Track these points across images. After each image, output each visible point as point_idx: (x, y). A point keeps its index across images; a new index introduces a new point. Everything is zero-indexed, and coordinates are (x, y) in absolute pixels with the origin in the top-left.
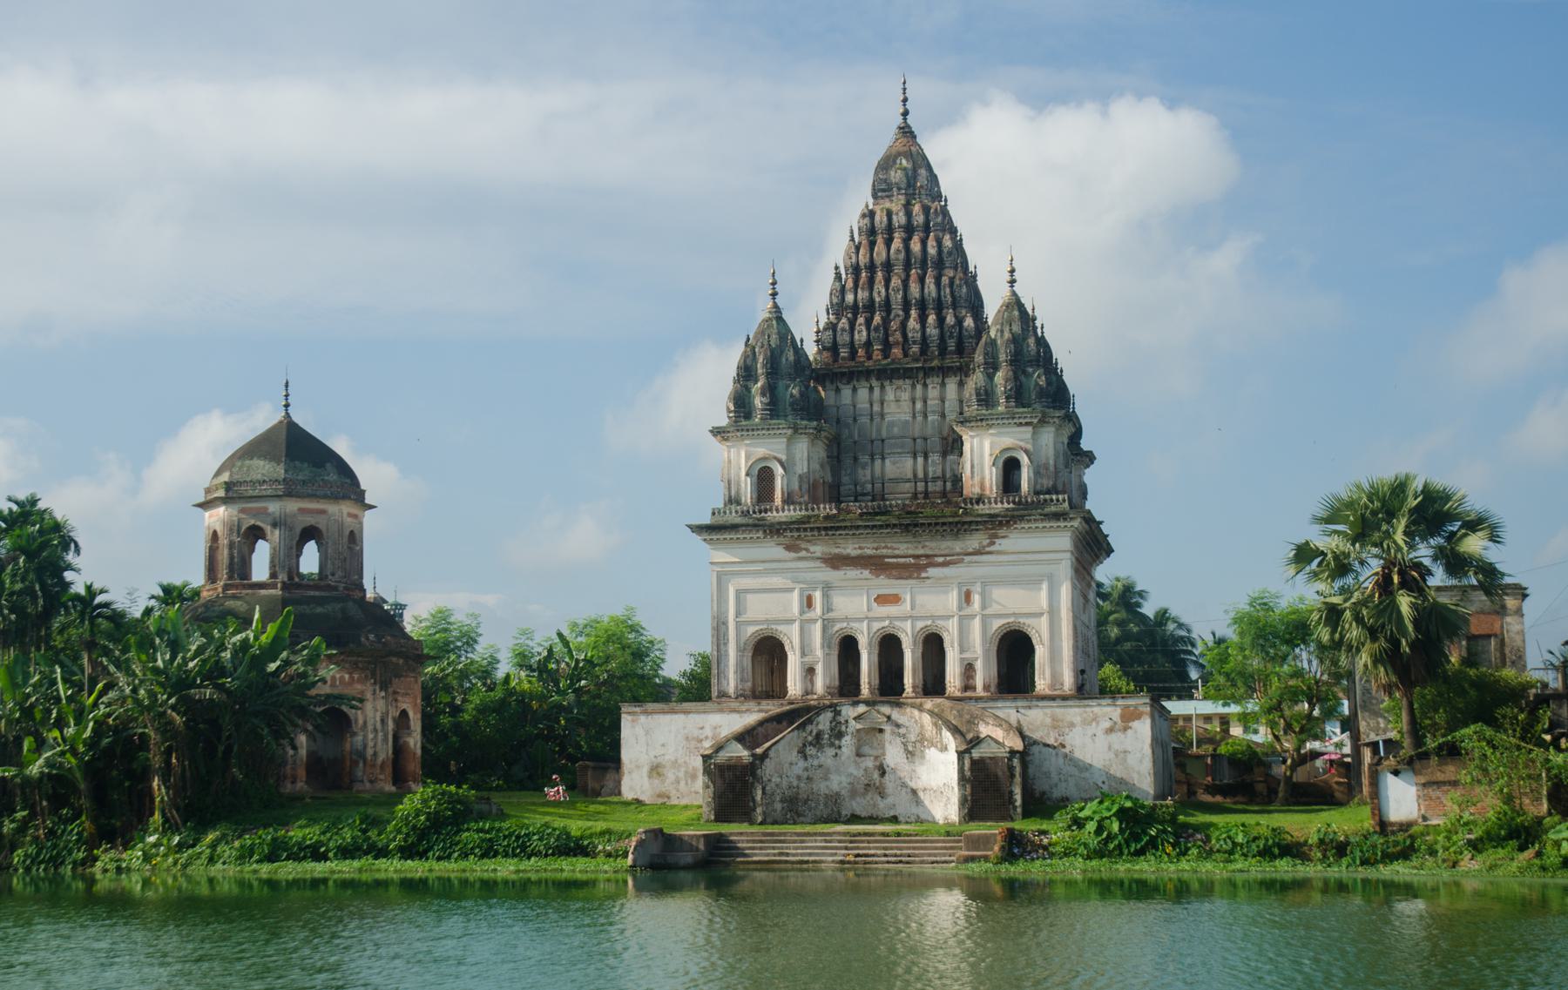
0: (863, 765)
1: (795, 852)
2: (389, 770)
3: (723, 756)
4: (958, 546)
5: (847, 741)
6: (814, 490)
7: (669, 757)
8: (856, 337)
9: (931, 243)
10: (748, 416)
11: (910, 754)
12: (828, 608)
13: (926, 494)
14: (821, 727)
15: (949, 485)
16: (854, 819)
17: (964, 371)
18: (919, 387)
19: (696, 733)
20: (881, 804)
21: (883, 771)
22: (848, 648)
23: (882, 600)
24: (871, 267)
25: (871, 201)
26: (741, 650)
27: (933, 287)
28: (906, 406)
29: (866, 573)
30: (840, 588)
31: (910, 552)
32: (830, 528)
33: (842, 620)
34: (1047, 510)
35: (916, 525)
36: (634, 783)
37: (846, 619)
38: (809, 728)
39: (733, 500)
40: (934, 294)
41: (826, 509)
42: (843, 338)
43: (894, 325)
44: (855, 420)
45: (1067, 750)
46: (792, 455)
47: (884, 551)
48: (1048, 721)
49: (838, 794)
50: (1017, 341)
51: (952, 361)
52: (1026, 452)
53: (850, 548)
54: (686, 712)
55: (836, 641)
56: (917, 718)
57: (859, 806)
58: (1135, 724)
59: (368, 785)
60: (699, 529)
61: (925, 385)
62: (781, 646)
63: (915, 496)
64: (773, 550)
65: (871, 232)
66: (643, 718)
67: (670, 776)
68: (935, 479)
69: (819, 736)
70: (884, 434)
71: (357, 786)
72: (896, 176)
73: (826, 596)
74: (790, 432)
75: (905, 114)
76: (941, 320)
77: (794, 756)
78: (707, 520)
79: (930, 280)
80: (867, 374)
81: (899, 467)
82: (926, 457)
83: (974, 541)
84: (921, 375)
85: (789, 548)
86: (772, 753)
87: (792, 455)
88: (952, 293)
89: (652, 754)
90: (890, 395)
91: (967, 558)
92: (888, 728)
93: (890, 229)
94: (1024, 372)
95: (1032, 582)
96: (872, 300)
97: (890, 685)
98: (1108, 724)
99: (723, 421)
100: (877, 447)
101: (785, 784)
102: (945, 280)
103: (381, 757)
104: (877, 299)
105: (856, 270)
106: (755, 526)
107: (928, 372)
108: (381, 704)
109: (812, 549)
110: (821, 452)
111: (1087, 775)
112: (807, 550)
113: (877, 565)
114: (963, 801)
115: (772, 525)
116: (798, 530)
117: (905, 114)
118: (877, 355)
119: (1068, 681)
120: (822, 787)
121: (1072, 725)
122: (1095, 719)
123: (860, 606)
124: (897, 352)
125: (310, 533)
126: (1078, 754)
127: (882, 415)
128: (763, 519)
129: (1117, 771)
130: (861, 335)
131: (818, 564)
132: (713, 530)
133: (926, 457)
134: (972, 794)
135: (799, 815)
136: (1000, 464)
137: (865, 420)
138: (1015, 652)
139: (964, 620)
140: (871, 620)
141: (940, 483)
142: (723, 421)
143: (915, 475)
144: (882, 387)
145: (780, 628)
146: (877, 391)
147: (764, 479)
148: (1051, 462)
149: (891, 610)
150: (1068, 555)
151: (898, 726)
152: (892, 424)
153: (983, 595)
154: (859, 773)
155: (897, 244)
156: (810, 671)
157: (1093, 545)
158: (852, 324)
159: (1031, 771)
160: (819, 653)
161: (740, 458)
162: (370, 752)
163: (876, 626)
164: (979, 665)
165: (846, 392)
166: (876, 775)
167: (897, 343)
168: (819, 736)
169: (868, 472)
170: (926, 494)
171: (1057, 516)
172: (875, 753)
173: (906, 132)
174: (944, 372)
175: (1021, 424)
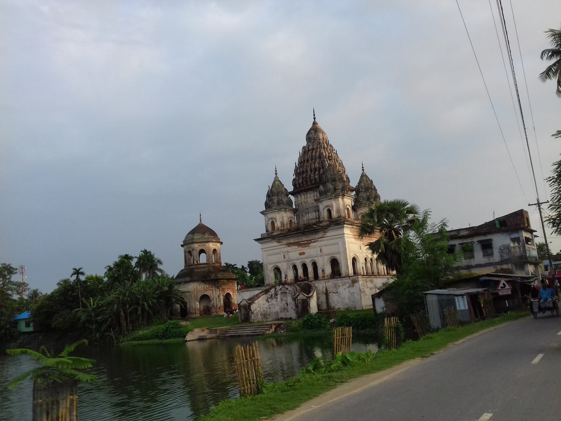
4: (317, 236)
5: (279, 296)
20: (287, 314)
22: (295, 267)
23: (302, 254)
28: (312, 198)
39: (267, 231)
40: (318, 166)
42: (297, 182)
47: (300, 240)
53: (292, 241)
58: (355, 284)
59: (215, 313)
60: (257, 240)
66: (241, 294)
69: (272, 295)
71: (213, 314)
75: (315, 119)
76: (319, 172)
77: (265, 302)
78: (260, 237)
83: (320, 235)
85: (278, 242)
88: (322, 166)
90: (309, 196)
93: (309, 150)
98: (348, 285)
101: (262, 310)
103: (219, 305)
108: (218, 293)
113: (298, 244)
117: (315, 119)
118: (305, 185)
120: (273, 310)
122: (345, 284)
124: (309, 183)
125: (202, 251)
130: (301, 181)
136: (326, 211)
147: (273, 223)
149: (303, 256)
154: (282, 305)
159: (330, 301)
162: (215, 305)
165: (299, 197)
166: (286, 306)
171: (338, 224)
173: (315, 123)
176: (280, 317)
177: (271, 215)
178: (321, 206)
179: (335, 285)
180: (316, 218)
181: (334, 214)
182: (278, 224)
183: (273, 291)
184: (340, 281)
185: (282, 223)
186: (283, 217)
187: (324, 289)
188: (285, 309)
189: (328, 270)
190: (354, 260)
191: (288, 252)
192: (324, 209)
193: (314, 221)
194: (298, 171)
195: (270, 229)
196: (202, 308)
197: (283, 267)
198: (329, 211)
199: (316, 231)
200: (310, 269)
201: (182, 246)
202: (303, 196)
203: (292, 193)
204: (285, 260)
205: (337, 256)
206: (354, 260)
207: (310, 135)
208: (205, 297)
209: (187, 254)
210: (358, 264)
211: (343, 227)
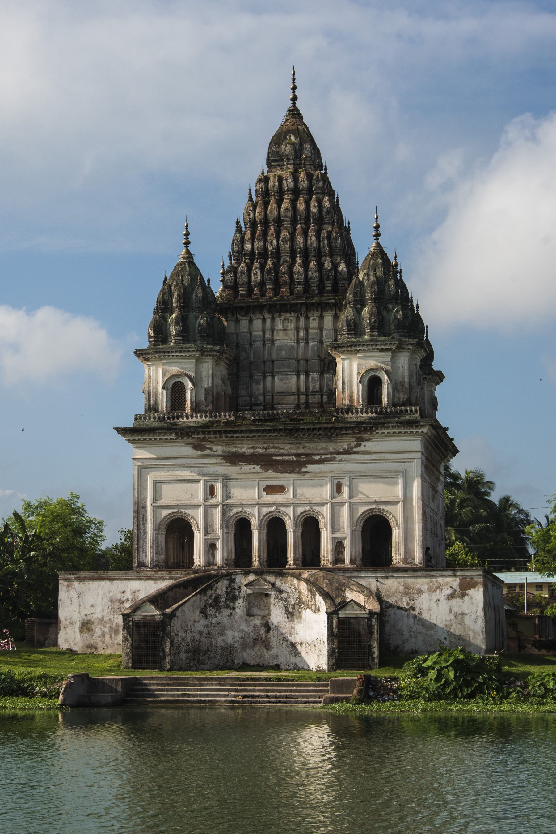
0: (252, 623)
1: (195, 693)
3: (140, 614)
4: (331, 447)
5: (240, 603)
6: (215, 401)
7: (98, 615)
8: (253, 278)
9: (313, 204)
10: (165, 340)
11: (291, 615)
12: (227, 496)
13: (307, 405)
14: (219, 592)
15: (325, 398)
16: (245, 667)
17: (338, 307)
18: (302, 319)
19: (119, 596)
21: (268, 627)
23: (270, 489)
24: (265, 222)
25: (266, 169)
26: (155, 529)
27: (314, 238)
28: (291, 334)
29: (258, 468)
30: (237, 480)
31: (293, 451)
32: (229, 432)
33: (237, 506)
34: (402, 419)
35: (298, 430)
36: (69, 637)
37: (241, 505)
38: (209, 593)
39: (152, 408)
40: (315, 245)
41: (226, 416)
43: (283, 269)
44: (251, 345)
45: (416, 612)
46: (198, 372)
47: (272, 450)
48: (402, 588)
49: (232, 646)
50: (380, 283)
51: (329, 298)
52: (386, 372)
53: (245, 449)
54: (111, 579)
55: (233, 522)
56: (297, 586)
57: (249, 656)
62: (189, 526)
63: (298, 406)
65: (265, 194)
66: (76, 584)
67: (98, 631)
68: (314, 393)
70: (274, 356)
72: (286, 149)
73: (225, 486)
74: (198, 354)
75: (294, 99)
76: (320, 265)
77: (197, 615)
78: (130, 423)
79: (311, 234)
80: (260, 308)
81: (286, 382)
82: (307, 375)
83: (343, 444)
84: (304, 309)
85: (196, 447)
86: (179, 613)
87: (198, 372)
89: (83, 612)
90: (279, 325)
91: (338, 457)
92: (272, 593)
93: (280, 192)
94: (386, 308)
95: (388, 477)
96: (265, 248)
99: (145, 344)
100: (269, 367)
101: (189, 638)
102: (324, 233)
104: (270, 248)
105: (253, 224)
106: (169, 429)
107: (309, 307)
109: (215, 448)
110: (223, 370)
112: (211, 449)
113: (267, 462)
114: (331, 653)
115: (182, 429)
116: (204, 433)
117: (294, 99)
118: (269, 293)
119: (418, 554)
120: (219, 640)
121: (420, 592)
122: (439, 587)
123: (250, 495)
124: (284, 290)
126: (425, 616)
127: (273, 341)
128: (176, 424)
129: (456, 630)
131: (219, 460)
132: (135, 433)
133: (307, 375)
134: (339, 647)
135: (200, 663)
137: (258, 345)
138: (375, 531)
139: (336, 506)
140: (261, 505)
141: (318, 396)
142: (145, 344)
143: (298, 389)
144: (273, 319)
145: (189, 511)
146: (268, 322)
148: (407, 380)
150: (419, 455)
151: (281, 591)
152: (280, 348)
153: (351, 487)
155: (286, 204)
157: (440, 447)
158: (249, 267)
159: (387, 628)
160: (219, 532)
161: (157, 374)
163: (265, 510)
164: (347, 543)
165: (244, 323)
166: (262, 632)
167: (285, 283)
168: (217, 599)
169: (261, 387)
170: (307, 405)
172: (262, 613)
174: (322, 307)
175: (382, 350)
179: (406, 587)
183: (221, 587)
207: (286, 149)
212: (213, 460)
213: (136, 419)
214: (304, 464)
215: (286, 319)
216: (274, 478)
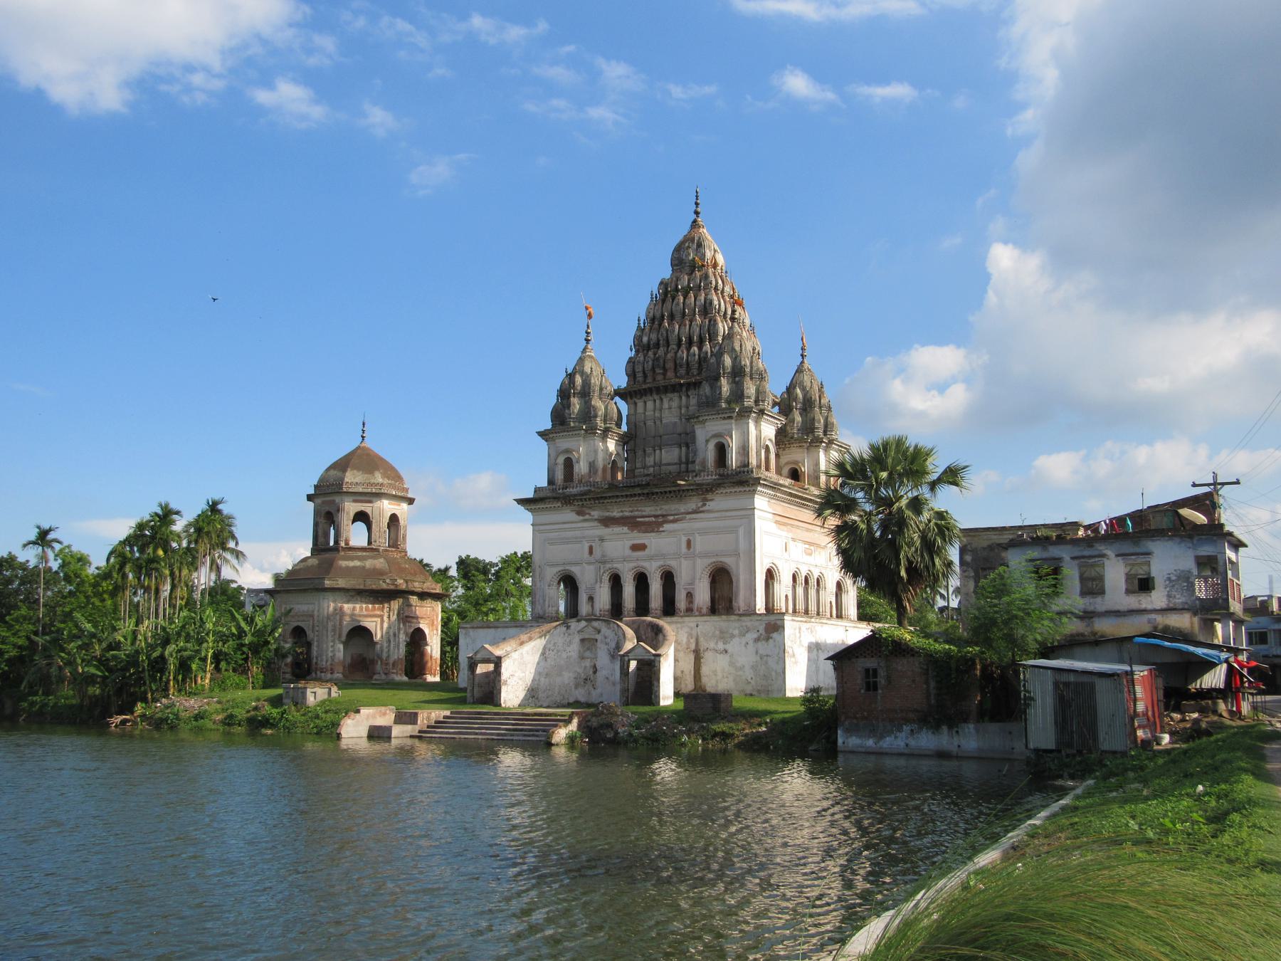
2: (402, 666)
22: (616, 581)
30: (610, 540)
39: (551, 482)
42: (639, 368)
53: (616, 513)
55: (606, 578)
58: (775, 635)
59: (383, 677)
60: (522, 502)
61: (688, 396)
64: (568, 515)
65: (666, 293)
71: (376, 677)
78: (530, 495)
82: (688, 446)
83: (693, 504)
85: (579, 513)
90: (666, 405)
97: (642, 607)
98: (755, 636)
107: (689, 386)
111: (740, 673)
113: (632, 523)
124: (670, 374)
131: (596, 524)
133: (688, 446)
136: (711, 446)
137: (650, 423)
156: (591, 599)
159: (705, 670)
162: (384, 655)
165: (640, 404)
171: (742, 483)
176: (571, 700)
177: (564, 443)
178: (701, 433)
179: (722, 632)
180: (680, 463)
181: (733, 460)
182: (581, 468)
184: (737, 625)
185: (592, 465)
186: (596, 452)
187: (693, 641)
188: (587, 680)
189: (703, 595)
190: (770, 575)
191: (602, 540)
192: (707, 441)
193: (673, 468)
194: (645, 339)
195: (560, 476)
196: (349, 660)
197: (586, 576)
198: (722, 450)
199: (680, 494)
200: (656, 588)
201: (310, 498)
202: (650, 405)
203: (620, 393)
204: (592, 559)
205: (729, 561)
206: (770, 575)
208: (360, 633)
209: (322, 520)
210: (776, 586)
211: (755, 491)
212: (592, 524)
213: (537, 490)
214: (661, 524)
215: (671, 399)
216: (639, 538)
